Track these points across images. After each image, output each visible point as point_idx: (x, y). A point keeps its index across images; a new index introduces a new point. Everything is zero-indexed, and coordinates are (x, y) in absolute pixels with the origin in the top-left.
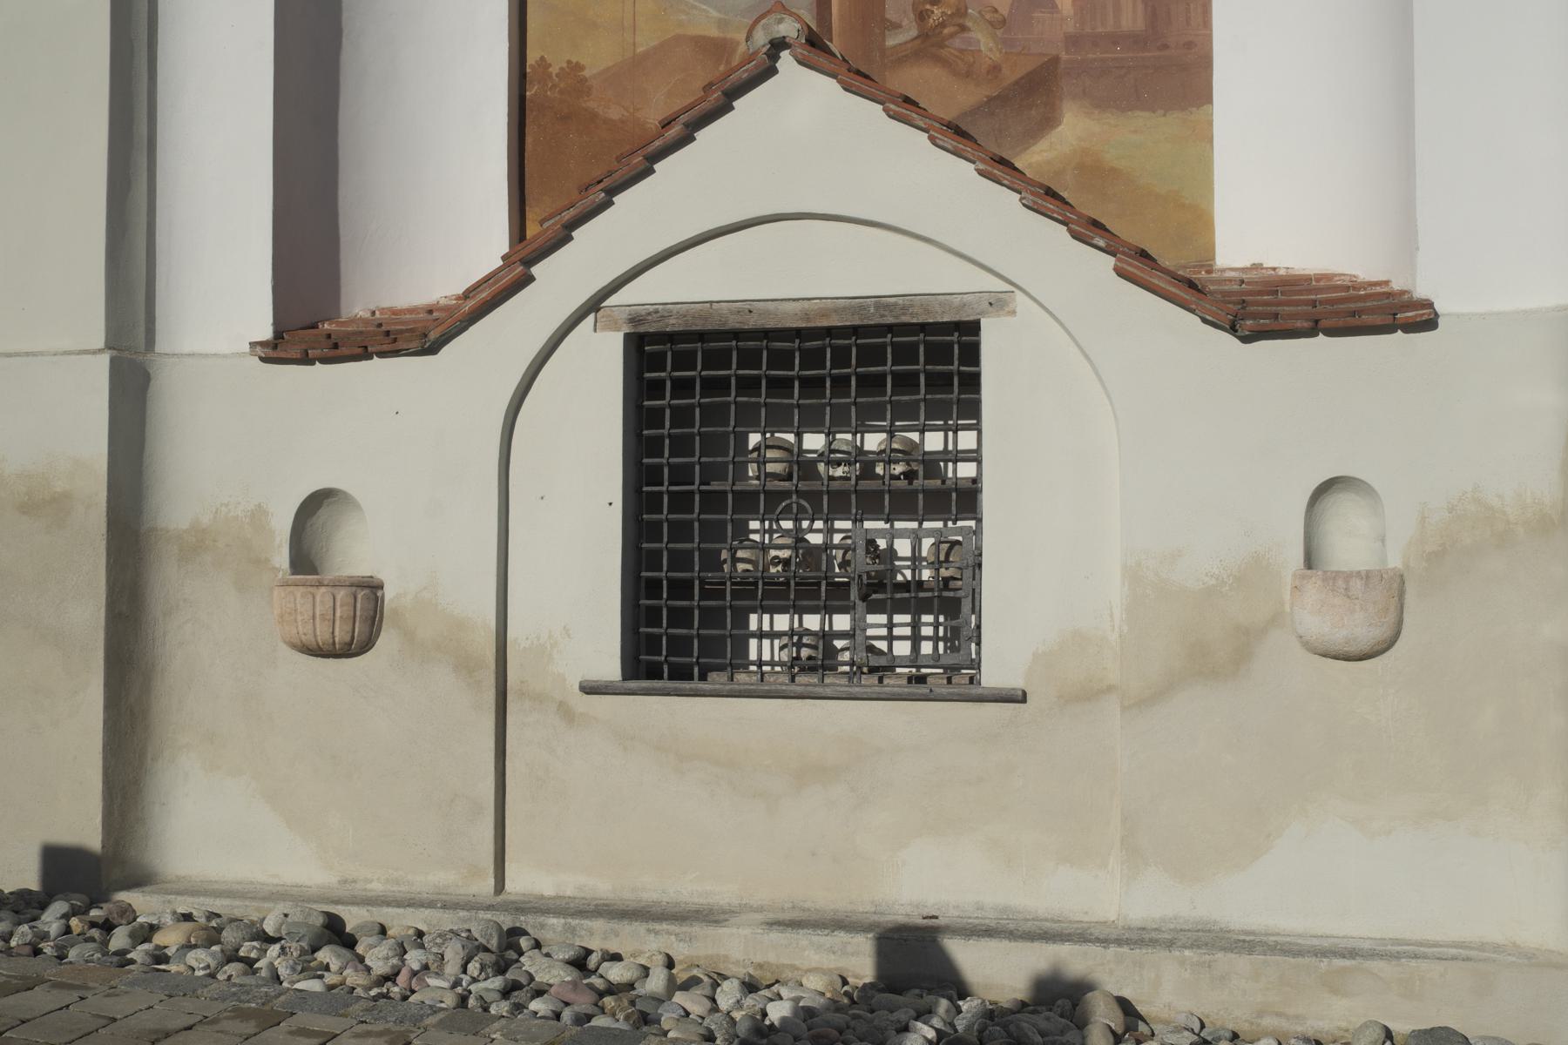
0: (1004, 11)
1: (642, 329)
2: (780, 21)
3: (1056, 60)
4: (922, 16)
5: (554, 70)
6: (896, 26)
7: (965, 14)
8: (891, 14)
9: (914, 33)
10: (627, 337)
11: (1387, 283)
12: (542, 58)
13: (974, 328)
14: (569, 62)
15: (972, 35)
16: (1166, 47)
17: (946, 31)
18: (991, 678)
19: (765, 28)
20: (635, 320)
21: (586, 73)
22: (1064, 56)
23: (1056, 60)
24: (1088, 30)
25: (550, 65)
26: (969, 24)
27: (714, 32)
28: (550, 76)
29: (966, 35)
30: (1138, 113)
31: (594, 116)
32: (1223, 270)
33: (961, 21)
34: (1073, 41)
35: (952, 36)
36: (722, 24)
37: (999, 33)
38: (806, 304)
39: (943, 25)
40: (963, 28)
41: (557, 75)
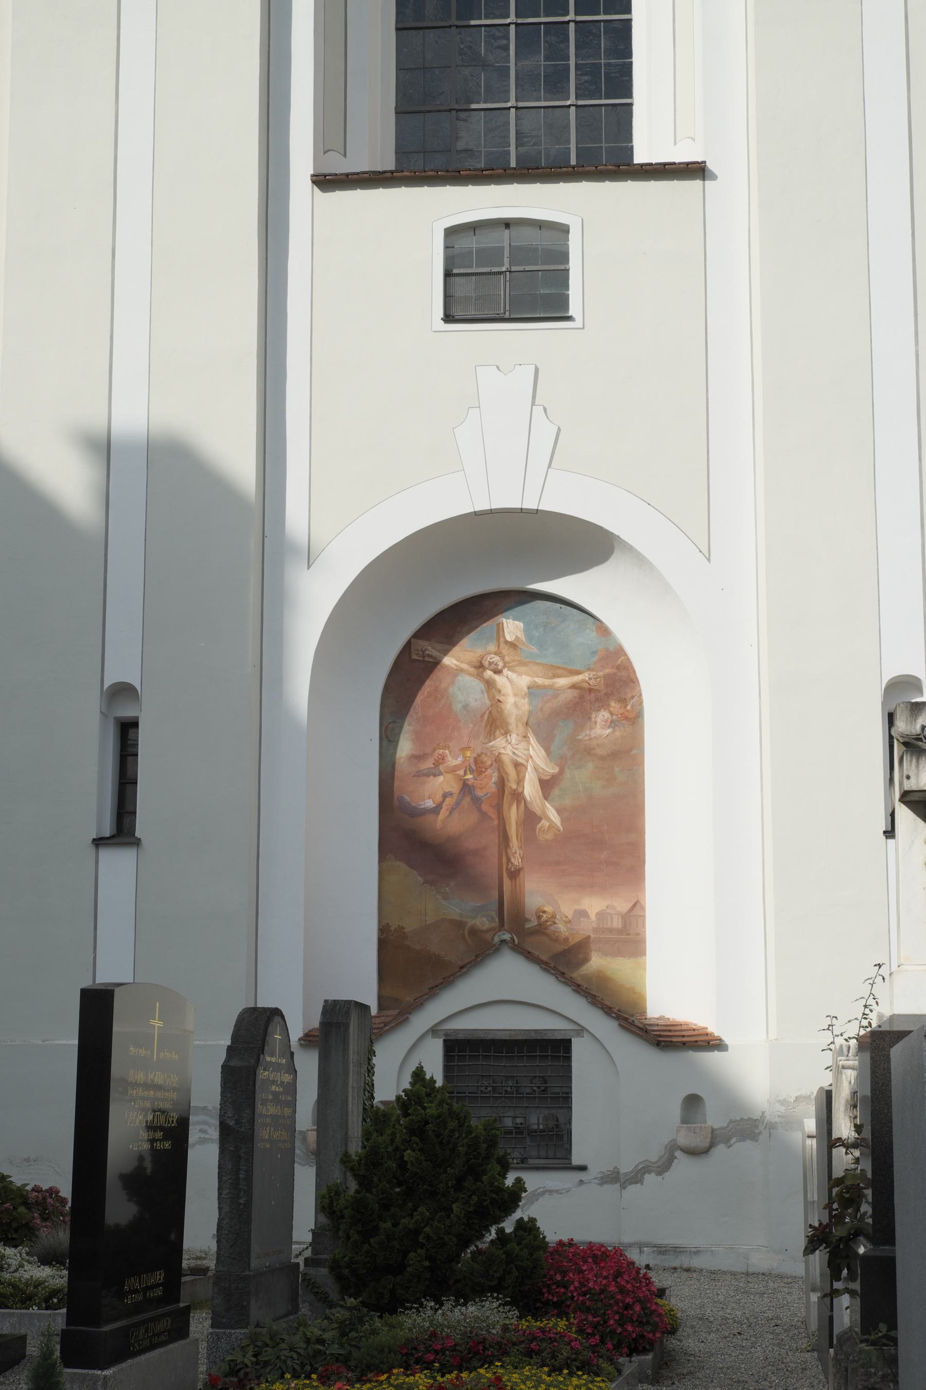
0: (570, 917)
1: (449, 1038)
2: (504, 934)
3: (589, 937)
5: (393, 928)
7: (555, 918)
10: (445, 1041)
11: (706, 1028)
12: (387, 923)
13: (569, 1041)
14: (399, 925)
15: (558, 925)
16: (629, 934)
17: (548, 923)
18: (576, 1160)
19: (499, 936)
21: (406, 930)
22: (592, 936)
24: (601, 926)
25: (390, 927)
26: (557, 921)
27: (458, 918)
28: (391, 930)
29: (555, 925)
30: (619, 958)
32: (650, 1019)
33: (553, 920)
34: (595, 930)
35: (550, 925)
37: (568, 925)
38: (510, 1032)
39: (547, 921)
41: (394, 930)
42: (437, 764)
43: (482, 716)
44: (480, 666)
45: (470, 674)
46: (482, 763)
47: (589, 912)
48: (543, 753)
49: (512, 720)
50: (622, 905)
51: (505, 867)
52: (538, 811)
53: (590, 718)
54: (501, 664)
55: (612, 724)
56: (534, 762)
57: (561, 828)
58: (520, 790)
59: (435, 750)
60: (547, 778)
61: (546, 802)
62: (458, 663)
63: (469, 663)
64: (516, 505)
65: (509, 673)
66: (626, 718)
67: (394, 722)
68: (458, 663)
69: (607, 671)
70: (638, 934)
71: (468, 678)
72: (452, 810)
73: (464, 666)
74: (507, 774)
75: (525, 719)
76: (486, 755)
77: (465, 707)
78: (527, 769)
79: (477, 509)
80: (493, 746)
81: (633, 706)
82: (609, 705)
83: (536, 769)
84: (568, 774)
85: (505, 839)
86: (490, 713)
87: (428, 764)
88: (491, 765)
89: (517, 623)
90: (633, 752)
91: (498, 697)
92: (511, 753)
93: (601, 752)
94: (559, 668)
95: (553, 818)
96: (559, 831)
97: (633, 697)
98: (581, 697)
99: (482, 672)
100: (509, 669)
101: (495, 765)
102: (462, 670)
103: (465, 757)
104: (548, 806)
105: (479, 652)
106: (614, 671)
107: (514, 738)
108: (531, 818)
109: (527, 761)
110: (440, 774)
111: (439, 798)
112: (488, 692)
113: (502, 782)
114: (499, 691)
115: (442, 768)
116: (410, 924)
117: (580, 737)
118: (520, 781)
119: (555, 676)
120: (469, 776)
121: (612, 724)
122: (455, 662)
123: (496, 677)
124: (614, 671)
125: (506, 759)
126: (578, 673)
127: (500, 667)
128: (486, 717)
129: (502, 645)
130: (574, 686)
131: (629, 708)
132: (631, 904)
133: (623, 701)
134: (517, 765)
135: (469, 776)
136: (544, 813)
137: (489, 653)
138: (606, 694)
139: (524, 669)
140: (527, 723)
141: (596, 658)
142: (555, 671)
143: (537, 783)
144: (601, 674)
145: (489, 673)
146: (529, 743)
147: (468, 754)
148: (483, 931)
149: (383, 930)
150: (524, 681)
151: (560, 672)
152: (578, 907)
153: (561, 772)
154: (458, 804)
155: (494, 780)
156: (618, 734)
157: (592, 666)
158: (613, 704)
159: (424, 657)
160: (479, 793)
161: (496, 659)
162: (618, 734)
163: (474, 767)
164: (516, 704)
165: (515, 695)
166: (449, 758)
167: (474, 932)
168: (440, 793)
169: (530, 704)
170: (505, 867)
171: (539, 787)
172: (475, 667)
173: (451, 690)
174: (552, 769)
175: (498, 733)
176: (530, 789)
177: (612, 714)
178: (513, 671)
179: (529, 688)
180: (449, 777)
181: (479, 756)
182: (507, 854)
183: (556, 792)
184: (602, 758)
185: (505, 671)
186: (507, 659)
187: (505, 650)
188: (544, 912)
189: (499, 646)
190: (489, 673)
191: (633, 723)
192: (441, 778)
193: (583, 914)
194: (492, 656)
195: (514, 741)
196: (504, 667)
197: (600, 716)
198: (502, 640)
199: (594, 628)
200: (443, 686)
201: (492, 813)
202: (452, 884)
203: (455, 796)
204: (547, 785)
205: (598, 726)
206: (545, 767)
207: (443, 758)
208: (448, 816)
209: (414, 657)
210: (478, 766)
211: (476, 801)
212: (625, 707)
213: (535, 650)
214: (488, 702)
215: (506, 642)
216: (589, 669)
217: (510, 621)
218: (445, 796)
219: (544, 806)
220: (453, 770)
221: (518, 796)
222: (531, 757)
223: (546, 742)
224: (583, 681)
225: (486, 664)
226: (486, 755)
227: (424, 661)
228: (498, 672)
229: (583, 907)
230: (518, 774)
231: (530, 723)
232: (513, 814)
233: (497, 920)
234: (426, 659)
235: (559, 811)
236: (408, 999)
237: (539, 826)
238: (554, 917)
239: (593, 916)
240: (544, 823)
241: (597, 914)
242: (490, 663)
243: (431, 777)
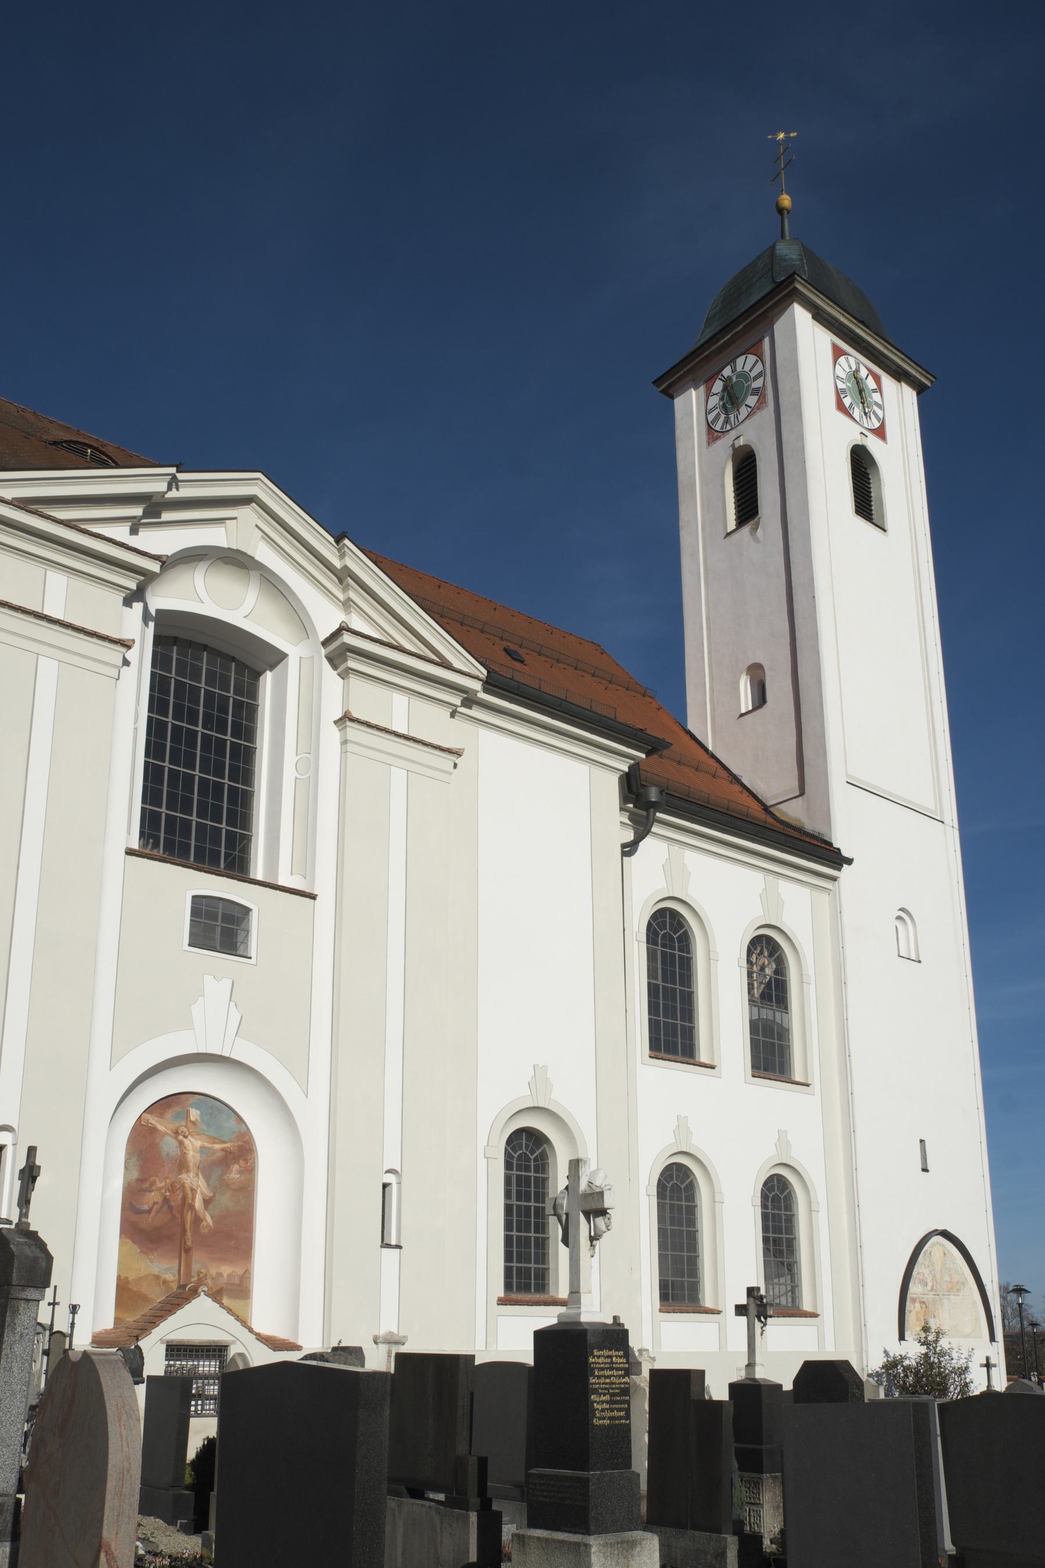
0: (214, 1276)
3: (223, 1288)
4: (199, 1275)
5: (122, 1278)
6: (193, 1277)
8: (193, 1274)
9: (197, 1279)
10: (167, 1345)
20: (167, 1342)
23: (223, 1288)
27: (157, 1273)
31: (130, 1289)
34: (226, 1284)
36: (159, 1272)
39: (202, 1278)
40: (206, 1279)
42: (151, 1185)
43: (176, 1161)
44: (176, 1133)
45: (171, 1136)
46: (175, 1187)
47: (224, 1273)
48: (206, 1184)
49: (191, 1164)
50: (240, 1271)
51: (183, 1246)
52: (201, 1216)
53: (230, 1168)
54: (187, 1133)
55: (240, 1172)
56: (201, 1189)
57: (212, 1227)
58: (193, 1204)
59: (150, 1177)
60: (207, 1198)
61: (206, 1213)
62: (166, 1130)
63: (171, 1130)
64: (219, 1053)
65: (191, 1139)
66: (247, 1170)
67: (130, 1159)
68: (166, 1130)
69: (240, 1143)
70: (246, 1287)
71: (170, 1138)
72: (157, 1212)
73: (169, 1132)
74: (187, 1194)
75: (198, 1164)
76: (177, 1182)
77: (168, 1154)
78: (197, 1192)
79: (200, 1052)
80: (181, 1178)
81: (251, 1164)
82: (239, 1162)
83: (202, 1193)
84: (217, 1197)
85: (184, 1230)
86: (180, 1160)
87: (147, 1185)
88: (179, 1188)
89: (197, 1111)
90: (249, 1189)
91: (184, 1151)
92: (189, 1182)
93: (233, 1187)
94: (216, 1139)
95: (208, 1220)
96: (211, 1228)
97: (251, 1159)
98: (226, 1156)
99: (177, 1136)
100: (192, 1136)
101: (181, 1188)
102: (167, 1134)
103: (166, 1182)
104: (207, 1214)
105: (177, 1124)
106: (243, 1144)
107: (191, 1175)
108: (198, 1220)
109: (197, 1188)
110: (152, 1191)
111: (151, 1205)
112: (180, 1147)
113: (184, 1198)
114: (186, 1148)
115: (154, 1188)
116: (132, 1276)
117: (224, 1178)
118: (194, 1199)
119: (214, 1143)
120: (168, 1194)
121: (240, 1172)
122: (164, 1129)
123: (185, 1140)
124: (243, 1144)
125: (187, 1186)
126: (225, 1142)
127: (187, 1134)
128: (178, 1161)
129: (189, 1122)
130: (223, 1150)
131: (249, 1164)
132: (244, 1271)
133: (246, 1161)
134: (192, 1190)
135: (168, 1194)
136: (205, 1218)
137: (182, 1126)
138: (238, 1156)
139: (198, 1137)
140: (198, 1167)
141: (234, 1136)
142: (214, 1140)
143: (202, 1201)
144: (236, 1144)
145: (181, 1137)
146: (199, 1178)
147: (168, 1181)
148: (169, 1282)
149: (119, 1278)
150: (198, 1144)
151: (216, 1141)
152: (218, 1271)
153: (214, 1196)
154: (161, 1208)
155: (180, 1197)
156: (242, 1178)
157: (233, 1140)
158: (241, 1161)
159: (148, 1123)
160: (173, 1204)
161: (185, 1130)
162: (242, 1178)
163: (170, 1188)
164: (193, 1155)
165: (193, 1151)
166: (158, 1182)
167: (165, 1282)
168: (152, 1202)
169: (201, 1156)
170: (183, 1246)
171: (202, 1203)
172: (174, 1133)
173: (161, 1144)
174: (210, 1194)
175: (183, 1171)
176: (198, 1204)
177: (240, 1167)
178: (193, 1137)
179: (201, 1148)
180: (157, 1193)
181: (174, 1182)
182: (184, 1239)
183: (211, 1206)
184: (234, 1190)
185: (189, 1137)
186: (191, 1130)
187: (190, 1126)
188: (201, 1273)
189: (187, 1123)
190: (181, 1137)
191: (250, 1173)
192: (153, 1194)
193: (220, 1275)
194: (183, 1128)
195: (191, 1177)
196: (189, 1134)
197: (235, 1168)
198: (189, 1119)
199: (234, 1119)
200: (157, 1141)
201: (178, 1216)
202: (155, 1254)
203: (160, 1204)
204: (207, 1202)
205: (233, 1172)
206: (206, 1193)
207: (153, 1183)
208: (155, 1216)
209: (143, 1123)
210: (172, 1188)
211: (170, 1208)
212: (247, 1163)
213: (205, 1127)
214: (179, 1153)
215: (191, 1121)
216: (231, 1141)
217: (194, 1109)
218: (154, 1204)
219: (204, 1213)
220: (161, 1188)
221: (192, 1207)
222: (200, 1186)
223: (207, 1179)
224: (227, 1147)
225: (180, 1132)
226: (177, 1182)
227: (147, 1126)
228: (186, 1137)
229: (221, 1271)
230: (193, 1194)
231: (200, 1167)
232: (189, 1217)
233: (177, 1275)
234: (149, 1125)
235: (212, 1217)
236: (128, 1319)
237: (201, 1225)
238: (206, 1275)
239: (225, 1276)
240: (204, 1223)
241: (228, 1275)
242: (182, 1132)
243: (148, 1193)
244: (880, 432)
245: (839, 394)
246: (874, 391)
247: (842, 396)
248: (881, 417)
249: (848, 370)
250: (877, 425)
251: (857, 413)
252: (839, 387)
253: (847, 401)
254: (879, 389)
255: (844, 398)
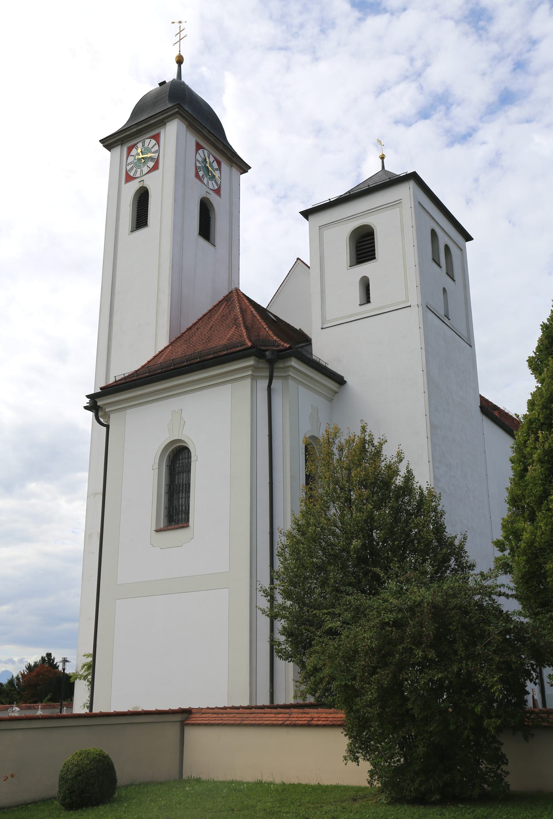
244: (218, 192)
245: (197, 169)
246: (216, 170)
247: (198, 171)
248: (219, 184)
249: (203, 157)
250: (216, 187)
251: (205, 181)
252: (197, 165)
253: (201, 173)
254: (220, 169)
255: (199, 171)
